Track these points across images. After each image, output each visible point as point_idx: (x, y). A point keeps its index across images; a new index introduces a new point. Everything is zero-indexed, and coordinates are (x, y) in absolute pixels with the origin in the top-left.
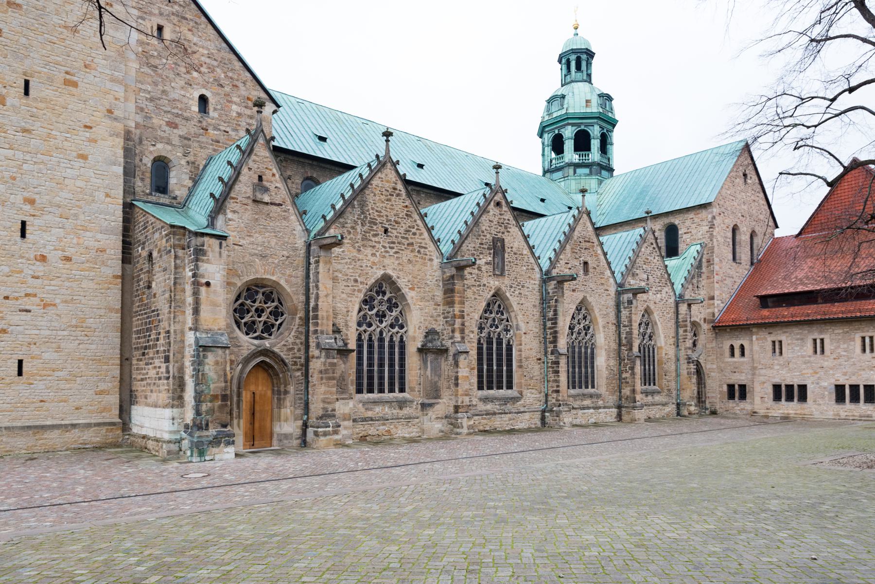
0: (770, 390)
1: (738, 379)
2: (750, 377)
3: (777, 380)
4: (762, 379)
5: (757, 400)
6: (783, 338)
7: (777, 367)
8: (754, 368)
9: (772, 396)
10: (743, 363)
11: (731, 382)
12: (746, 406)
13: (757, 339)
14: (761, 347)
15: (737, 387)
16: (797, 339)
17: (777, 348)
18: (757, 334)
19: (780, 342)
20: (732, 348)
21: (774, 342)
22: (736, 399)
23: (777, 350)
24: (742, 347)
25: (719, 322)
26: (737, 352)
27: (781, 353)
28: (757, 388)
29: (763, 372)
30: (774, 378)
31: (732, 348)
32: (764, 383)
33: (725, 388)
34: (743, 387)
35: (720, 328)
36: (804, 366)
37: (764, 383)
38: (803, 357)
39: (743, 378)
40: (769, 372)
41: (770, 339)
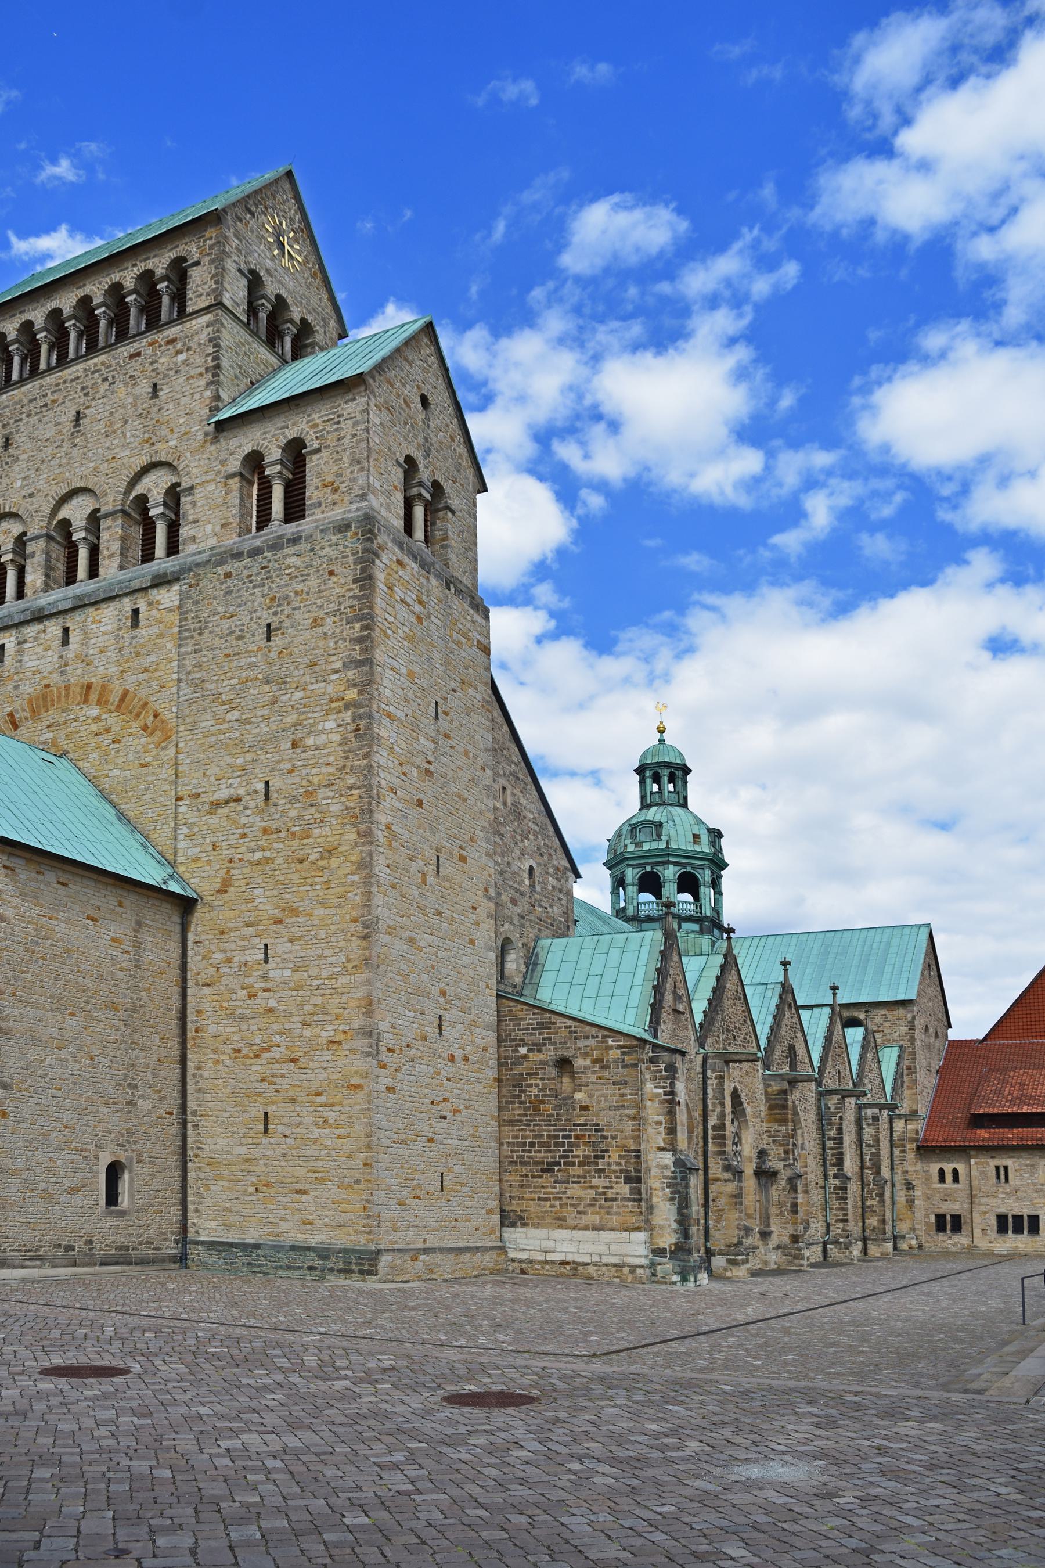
0: (994, 1221)
1: (950, 1208)
2: (966, 1206)
3: (1002, 1210)
4: (983, 1208)
5: (977, 1232)
6: (1009, 1162)
7: (1001, 1196)
8: (972, 1196)
9: (995, 1228)
10: (957, 1190)
11: (941, 1212)
12: (962, 1240)
13: (976, 1163)
14: (982, 1172)
15: (948, 1217)
16: (1027, 1165)
17: (1002, 1174)
18: (976, 1157)
19: (1006, 1168)
20: (942, 1173)
21: (997, 1168)
22: (948, 1232)
23: (1002, 1177)
24: (955, 1173)
25: (925, 1140)
26: (949, 1177)
27: (1007, 1180)
28: (977, 1218)
29: (983, 1200)
30: (999, 1207)
31: (942, 1173)
32: (986, 1213)
33: (933, 1219)
34: (957, 1220)
35: (925, 1150)
36: (1035, 1195)
37: (986, 1213)
38: (1034, 1184)
39: (957, 1207)
40: (992, 1201)
41: (993, 1163)
